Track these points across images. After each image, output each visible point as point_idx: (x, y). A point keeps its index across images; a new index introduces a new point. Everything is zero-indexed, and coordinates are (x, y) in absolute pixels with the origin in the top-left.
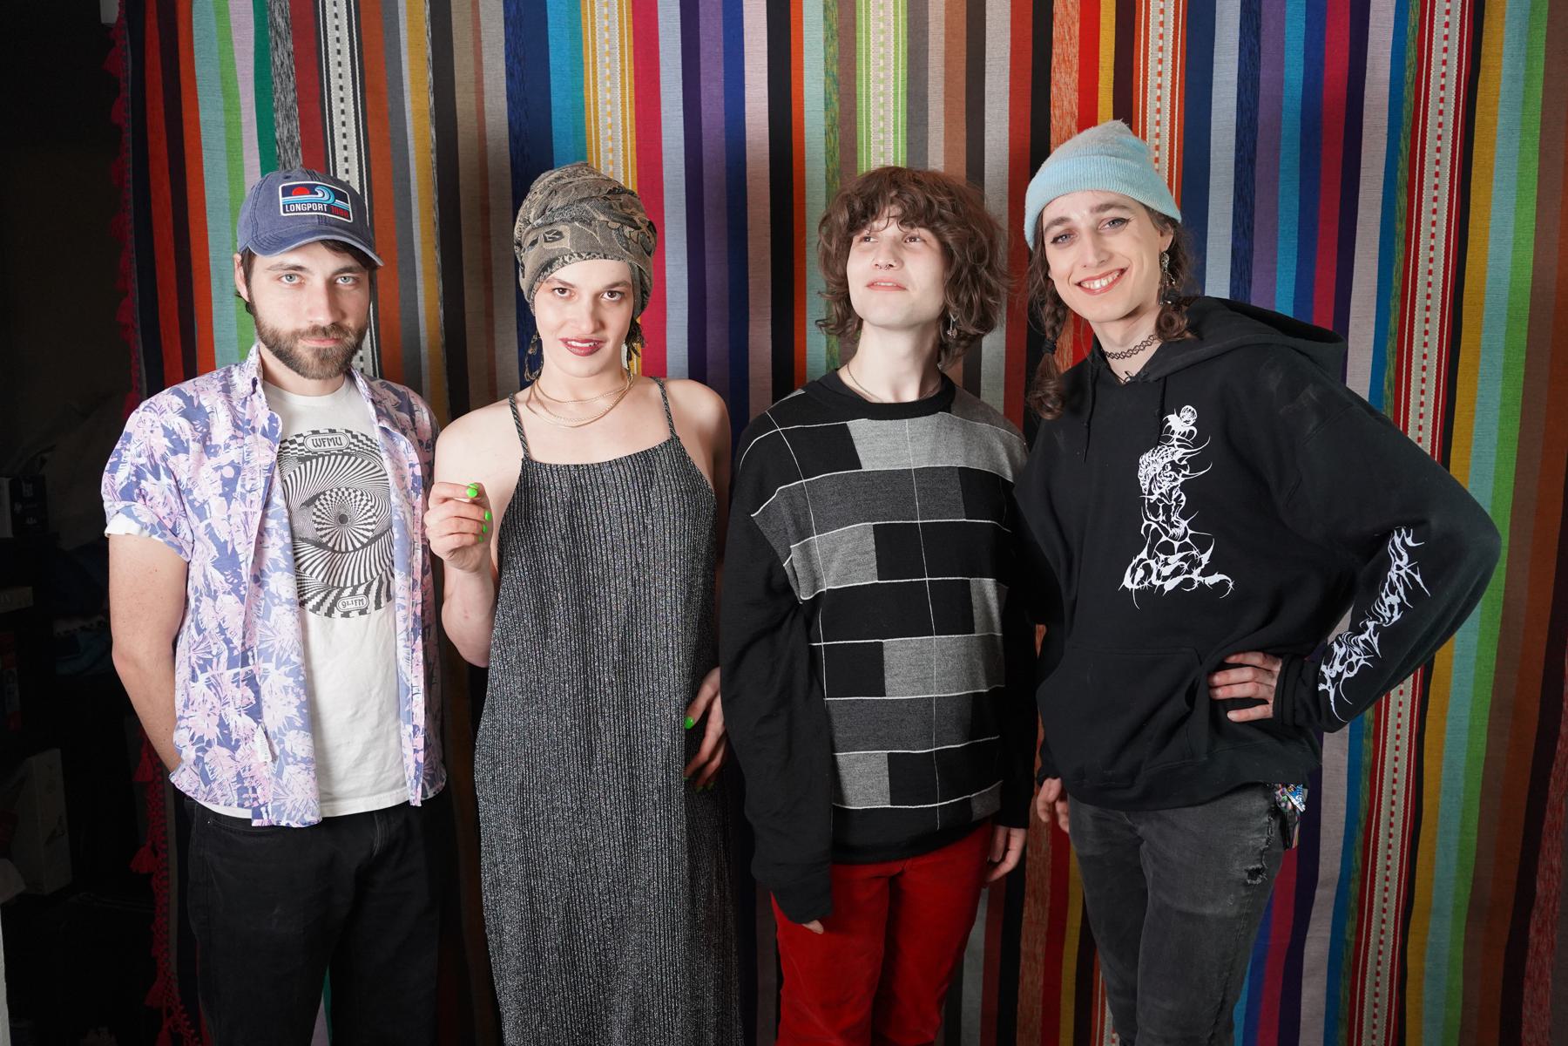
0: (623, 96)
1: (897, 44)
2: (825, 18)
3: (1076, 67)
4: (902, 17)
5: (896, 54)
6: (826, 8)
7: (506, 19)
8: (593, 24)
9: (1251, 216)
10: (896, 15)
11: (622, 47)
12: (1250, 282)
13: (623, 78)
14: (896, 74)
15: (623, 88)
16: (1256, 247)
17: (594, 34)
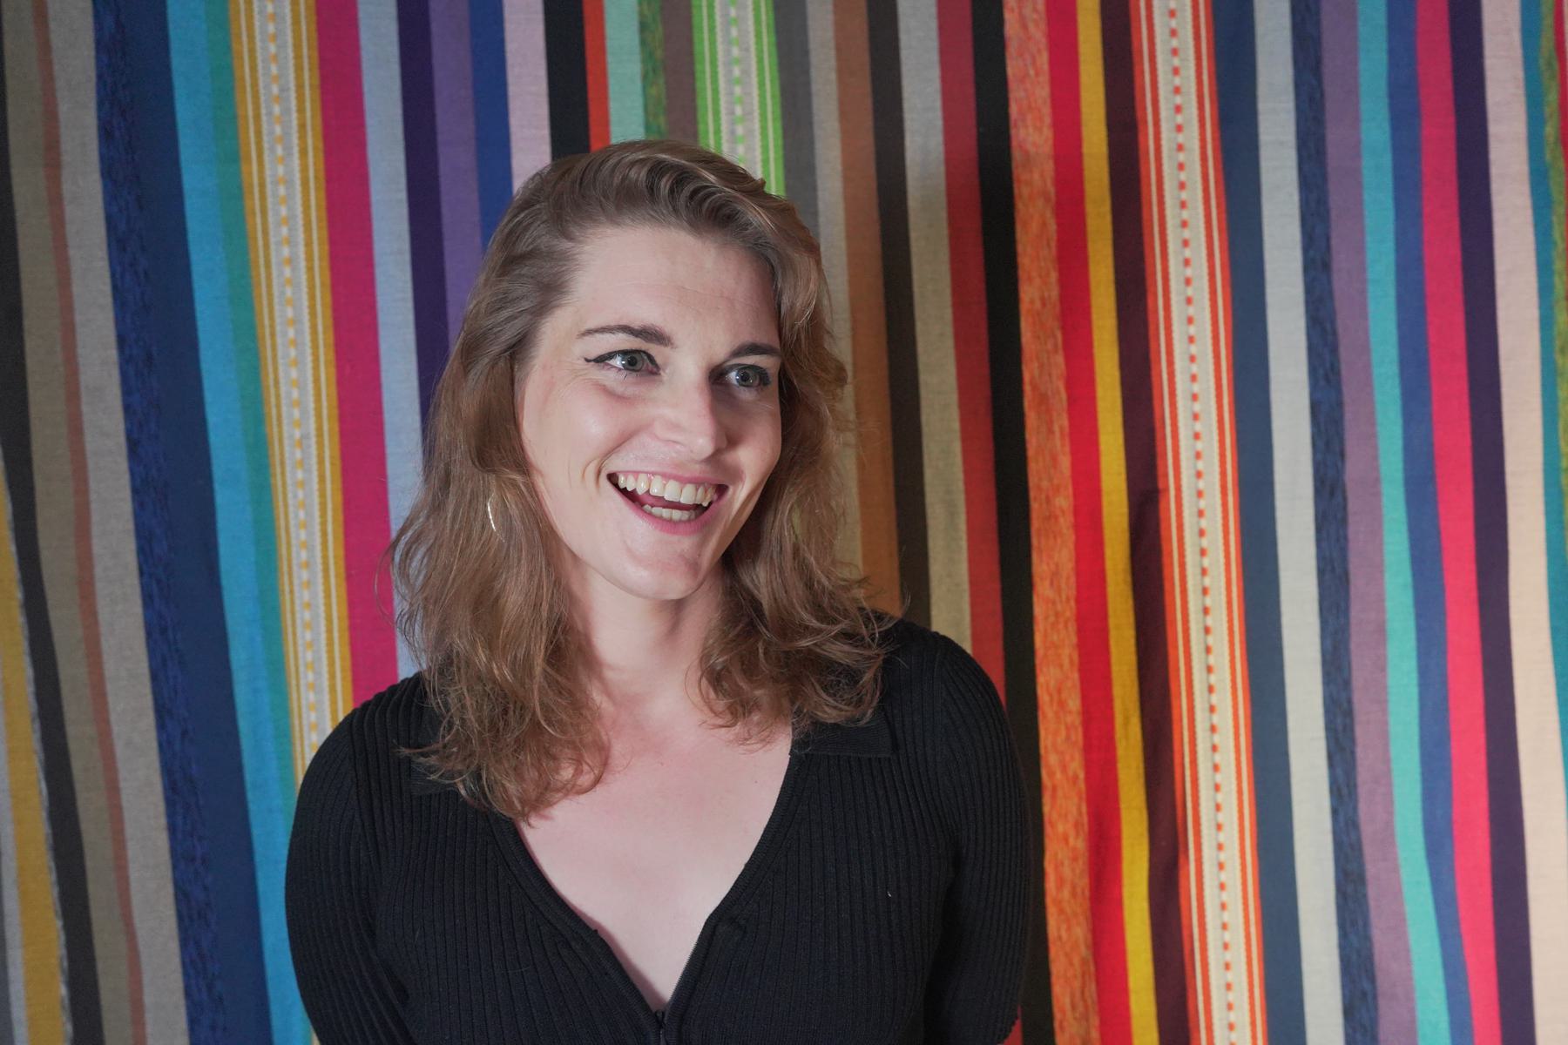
0: (304, 169)
1: (762, 85)
2: (643, 43)
3: (1048, 120)
4: (768, 39)
5: (762, 96)
6: (643, 27)
7: (98, 42)
8: (252, 51)
9: (1334, 350)
10: (758, 35)
11: (300, 87)
12: (1342, 454)
13: (302, 137)
14: (764, 129)
15: (303, 152)
16: (1347, 398)
17: (253, 69)
